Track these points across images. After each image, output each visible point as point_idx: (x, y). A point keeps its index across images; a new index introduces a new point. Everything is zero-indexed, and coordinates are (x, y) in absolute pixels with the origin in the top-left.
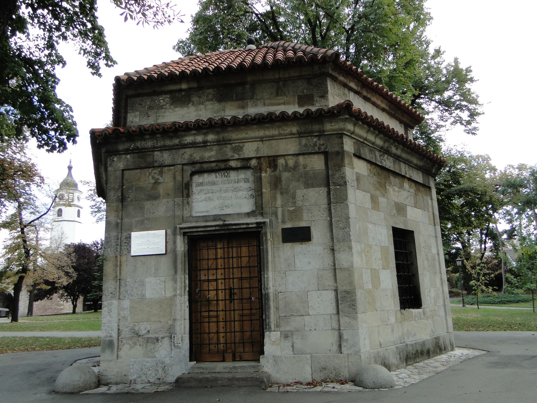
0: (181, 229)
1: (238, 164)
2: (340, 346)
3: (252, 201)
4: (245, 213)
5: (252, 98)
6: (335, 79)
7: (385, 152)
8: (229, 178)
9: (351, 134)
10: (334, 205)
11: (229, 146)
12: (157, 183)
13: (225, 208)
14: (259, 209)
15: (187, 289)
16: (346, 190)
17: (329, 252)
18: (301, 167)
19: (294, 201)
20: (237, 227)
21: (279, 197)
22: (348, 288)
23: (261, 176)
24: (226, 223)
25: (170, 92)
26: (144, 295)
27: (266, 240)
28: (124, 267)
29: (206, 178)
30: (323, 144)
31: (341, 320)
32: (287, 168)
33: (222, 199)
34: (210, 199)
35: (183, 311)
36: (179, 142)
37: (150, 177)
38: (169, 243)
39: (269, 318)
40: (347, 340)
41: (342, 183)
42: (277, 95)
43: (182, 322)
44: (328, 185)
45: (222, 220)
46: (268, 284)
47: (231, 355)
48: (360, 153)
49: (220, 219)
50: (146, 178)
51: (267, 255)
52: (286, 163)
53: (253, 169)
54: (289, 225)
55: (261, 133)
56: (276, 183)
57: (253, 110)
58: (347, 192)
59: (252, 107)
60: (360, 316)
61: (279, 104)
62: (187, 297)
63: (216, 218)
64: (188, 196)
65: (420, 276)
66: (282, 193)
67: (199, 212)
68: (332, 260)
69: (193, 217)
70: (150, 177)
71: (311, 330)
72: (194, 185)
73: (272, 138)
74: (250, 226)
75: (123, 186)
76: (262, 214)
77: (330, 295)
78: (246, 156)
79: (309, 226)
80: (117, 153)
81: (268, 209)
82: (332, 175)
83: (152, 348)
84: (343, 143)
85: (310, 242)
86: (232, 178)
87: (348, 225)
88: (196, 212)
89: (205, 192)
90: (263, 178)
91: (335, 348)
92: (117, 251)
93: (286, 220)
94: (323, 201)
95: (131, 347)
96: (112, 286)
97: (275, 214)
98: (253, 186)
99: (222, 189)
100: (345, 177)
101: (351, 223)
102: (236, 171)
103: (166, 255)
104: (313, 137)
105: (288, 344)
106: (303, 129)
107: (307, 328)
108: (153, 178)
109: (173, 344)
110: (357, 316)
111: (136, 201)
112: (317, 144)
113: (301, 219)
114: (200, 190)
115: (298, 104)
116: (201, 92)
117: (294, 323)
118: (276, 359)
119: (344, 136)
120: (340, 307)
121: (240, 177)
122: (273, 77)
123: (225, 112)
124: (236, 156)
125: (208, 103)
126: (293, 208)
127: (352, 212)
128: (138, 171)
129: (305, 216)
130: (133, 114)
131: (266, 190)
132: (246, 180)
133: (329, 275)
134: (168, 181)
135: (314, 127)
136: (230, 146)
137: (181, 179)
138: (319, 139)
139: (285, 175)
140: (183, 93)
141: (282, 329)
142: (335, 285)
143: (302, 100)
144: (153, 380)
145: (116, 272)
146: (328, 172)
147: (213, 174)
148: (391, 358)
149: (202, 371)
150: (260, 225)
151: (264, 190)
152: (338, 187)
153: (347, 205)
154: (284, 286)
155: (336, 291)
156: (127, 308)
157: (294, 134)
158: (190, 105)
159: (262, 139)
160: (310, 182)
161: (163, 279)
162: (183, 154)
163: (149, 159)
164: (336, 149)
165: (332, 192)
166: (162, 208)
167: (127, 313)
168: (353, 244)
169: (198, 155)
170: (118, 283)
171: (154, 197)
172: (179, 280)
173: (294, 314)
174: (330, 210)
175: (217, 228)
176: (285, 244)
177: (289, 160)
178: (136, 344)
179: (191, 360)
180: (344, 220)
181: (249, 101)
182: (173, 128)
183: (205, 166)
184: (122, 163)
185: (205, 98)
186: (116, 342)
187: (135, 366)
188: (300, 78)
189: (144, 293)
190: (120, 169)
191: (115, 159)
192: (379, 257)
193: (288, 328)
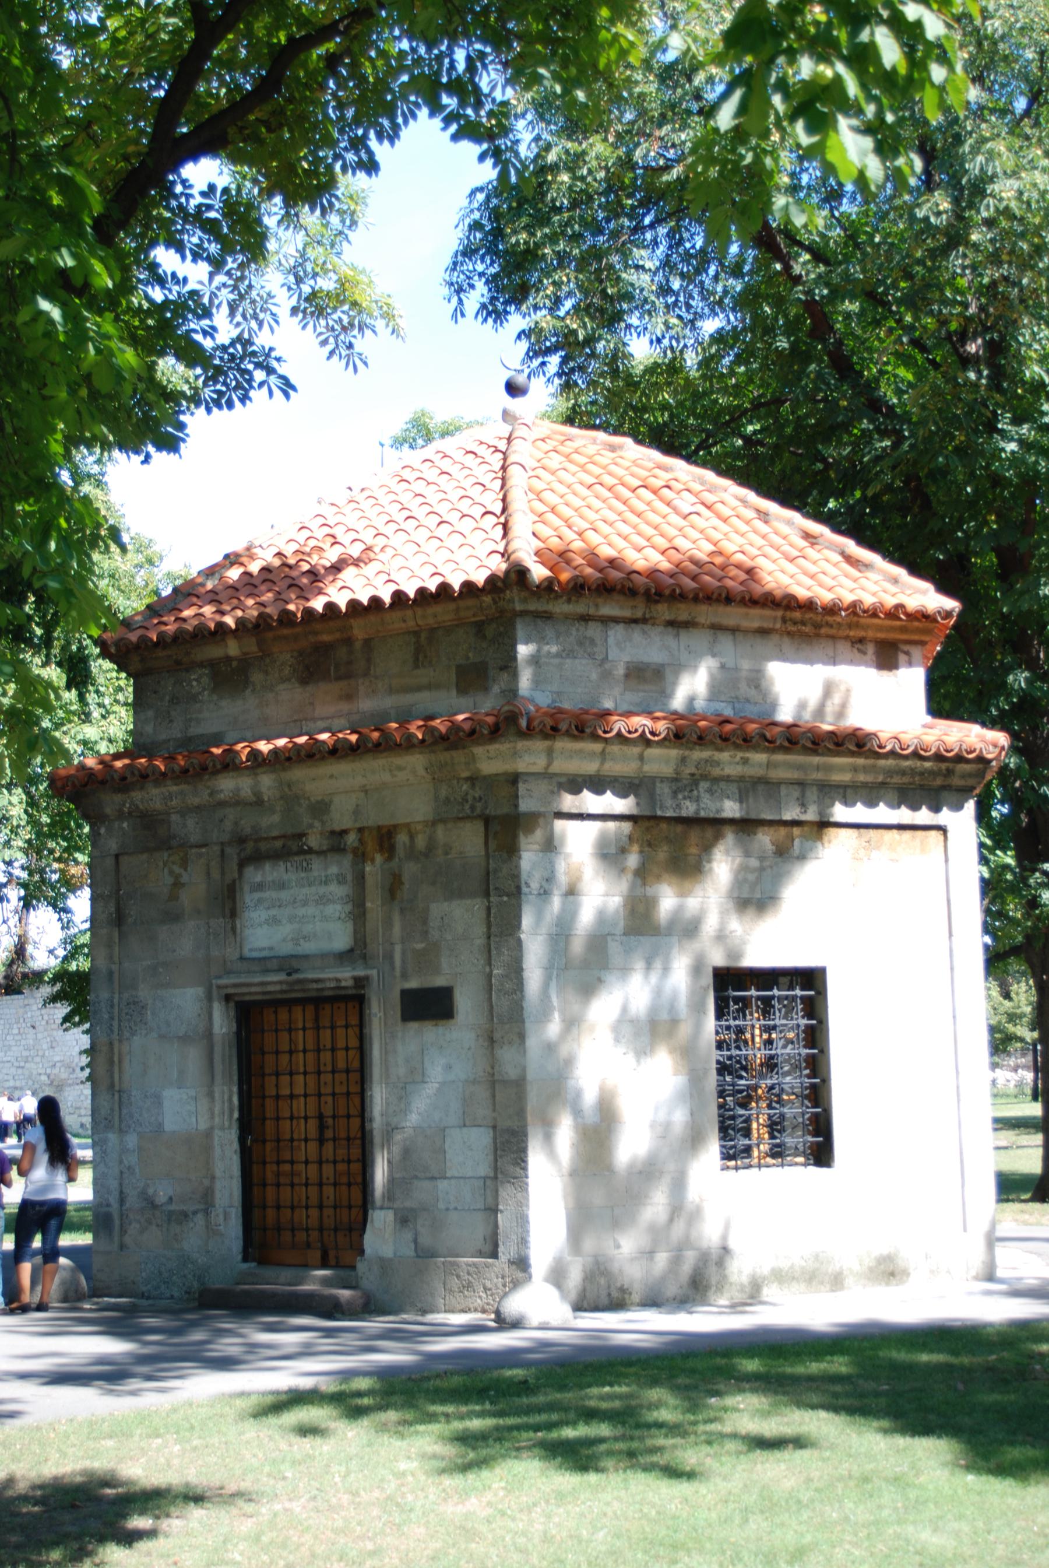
0: (219, 987)
5: (366, 674)
12: (177, 884)
13: (302, 941)
15: (236, 1115)
18: (440, 851)
20: (320, 986)
25: (212, 664)
26: (161, 1125)
30: (480, 798)
34: (275, 921)
36: (211, 795)
42: (416, 666)
44: (487, 894)
47: (318, 1254)
54: (413, 984)
56: (393, 888)
61: (419, 688)
64: (233, 914)
66: (402, 911)
72: (247, 888)
76: (364, 957)
82: (496, 871)
84: (517, 797)
86: (316, 874)
88: (251, 950)
94: (479, 931)
97: (389, 957)
107: (441, 1205)
108: (171, 872)
112: (470, 798)
113: (437, 971)
125: (281, 687)
128: (145, 856)
129: (445, 962)
131: (374, 904)
132: (341, 880)
133: (482, 1093)
139: (410, 869)
145: (112, 1077)
150: (361, 982)
151: (368, 905)
152: (505, 899)
155: (494, 1127)
158: (248, 692)
165: (493, 911)
166: (185, 941)
167: (132, 1159)
171: (173, 917)
172: (217, 1095)
179: (245, 1259)
181: (360, 681)
183: (263, 846)
193: (408, 1204)
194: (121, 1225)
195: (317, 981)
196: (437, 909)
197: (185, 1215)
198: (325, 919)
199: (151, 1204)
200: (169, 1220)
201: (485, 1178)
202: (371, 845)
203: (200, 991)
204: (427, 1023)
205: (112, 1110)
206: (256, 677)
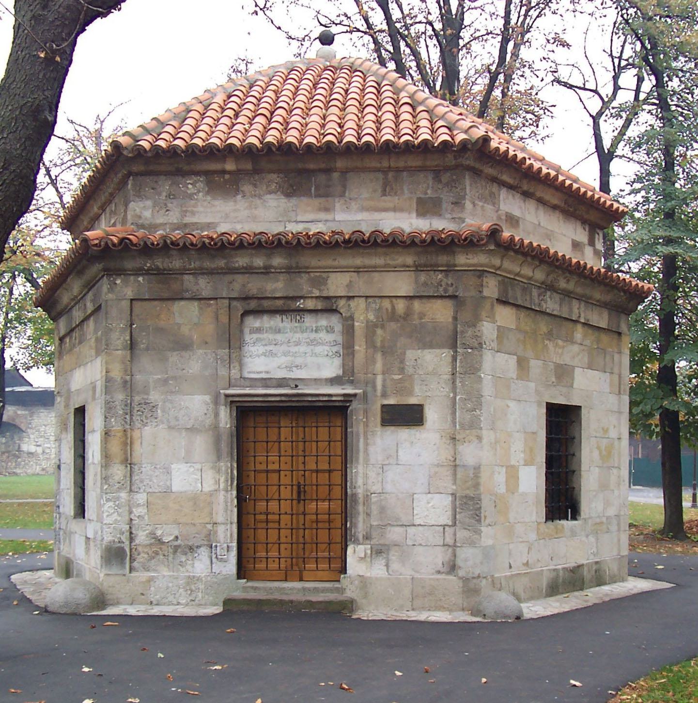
0: (227, 396)
1: (320, 305)
3: (338, 362)
4: (326, 380)
5: (342, 195)
8: (303, 325)
9: (496, 270)
10: (462, 376)
11: (305, 277)
13: (294, 369)
16: (481, 356)
17: (448, 442)
18: (416, 316)
19: (402, 366)
23: (353, 326)
25: (207, 173)
30: (452, 284)
33: (292, 356)
34: (271, 354)
35: (229, 512)
39: (356, 527)
41: (476, 345)
42: (384, 194)
43: (229, 526)
46: (356, 483)
51: (358, 441)
54: (391, 401)
55: (358, 261)
62: (235, 493)
63: (282, 382)
67: (254, 372)
68: (452, 453)
69: (244, 378)
71: (414, 545)
72: (246, 330)
73: (374, 269)
74: (334, 399)
75: (131, 325)
76: (352, 382)
81: (360, 376)
82: (462, 332)
85: (421, 427)
86: (307, 324)
88: (249, 372)
90: (356, 328)
92: (126, 422)
93: (389, 393)
96: (119, 472)
98: (340, 339)
99: (291, 341)
104: (437, 273)
106: (423, 260)
109: (214, 556)
112: (443, 284)
113: (411, 393)
114: (257, 339)
116: (257, 177)
120: (457, 517)
122: (378, 165)
123: (297, 215)
124: (317, 293)
125: (268, 196)
126: (400, 376)
127: (487, 388)
129: (417, 389)
130: (141, 204)
131: (360, 347)
132: (330, 330)
133: (446, 473)
135: (440, 258)
136: (307, 276)
138: (447, 276)
140: (227, 176)
147: (278, 316)
150: (349, 398)
151: (357, 348)
152: (470, 351)
154: (380, 484)
157: (408, 267)
158: (239, 197)
159: (358, 270)
161: (198, 466)
162: (231, 283)
163: (175, 286)
165: (459, 358)
166: (195, 364)
168: (485, 433)
169: (254, 285)
170: (129, 468)
174: (454, 382)
175: (283, 399)
181: (337, 200)
183: (266, 304)
188: (423, 169)
194: (131, 555)
196: (411, 355)
200: (175, 552)
201: (444, 526)
203: (207, 398)
204: (400, 427)
205: (125, 477)
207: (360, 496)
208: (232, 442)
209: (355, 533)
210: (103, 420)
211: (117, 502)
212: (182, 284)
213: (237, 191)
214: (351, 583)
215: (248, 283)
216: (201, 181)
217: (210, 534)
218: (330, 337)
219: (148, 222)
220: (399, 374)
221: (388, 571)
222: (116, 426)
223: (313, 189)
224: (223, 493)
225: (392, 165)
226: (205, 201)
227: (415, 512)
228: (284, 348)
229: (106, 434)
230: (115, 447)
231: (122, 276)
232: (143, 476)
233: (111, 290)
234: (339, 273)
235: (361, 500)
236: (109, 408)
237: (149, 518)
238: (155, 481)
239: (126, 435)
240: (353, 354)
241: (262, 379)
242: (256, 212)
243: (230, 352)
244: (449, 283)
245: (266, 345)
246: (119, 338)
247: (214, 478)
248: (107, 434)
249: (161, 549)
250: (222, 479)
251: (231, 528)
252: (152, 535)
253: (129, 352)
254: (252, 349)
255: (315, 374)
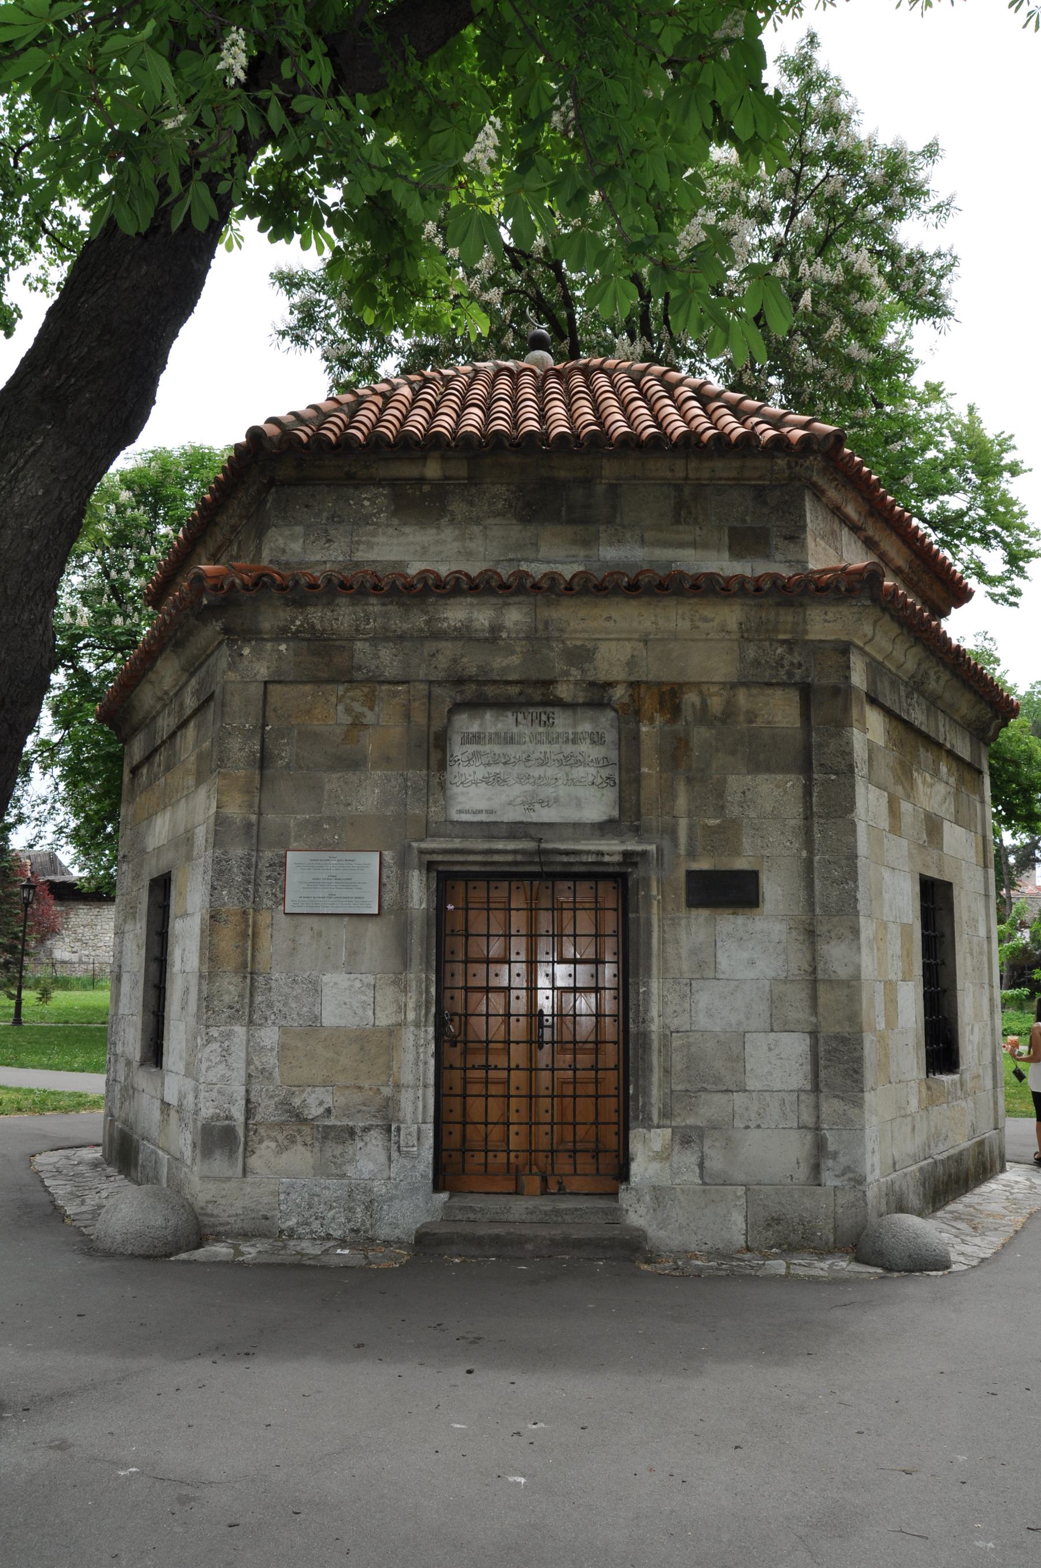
0: (422, 852)
2: (816, 1169)
3: (610, 795)
4: (593, 825)
5: (610, 521)
6: (818, 494)
7: (917, 686)
13: (537, 806)
14: (629, 817)
15: (433, 1010)
16: (853, 787)
17: (801, 938)
18: (741, 718)
20: (572, 859)
21: (682, 789)
22: (846, 1030)
23: (638, 731)
24: (543, 845)
25: (393, 483)
26: (317, 1018)
27: (648, 897)
28: (264, 941)
29: (490, 722)
30: (800, 665)
31: (825, 1107)
32: (704, 716)
34: (497, 780)
36: (428, 622)
37: (340, 707)
38: (389, 887)
39: (647, 1093)
40: (835, 1155)
42: (677, 520)
43: (420, 1093)
45: (533, 839)
46: (646, 1011)
47: (537, 1181)
48: (875, 692)
49: (527, 836)
50: (332, 712)
52: (704, 703)
53: (615, 710)
54: (704, 865)
56: (676, 753)
57: (616, 553)
58: (854, 791)
59: (611, 544)
60: (868, 1096)
61: (681, 545)
62: (431, 1030)
63: (516, 830)
64: (443, 766)
65: (959, 994)
66: (689, 781)
67: (467, 812)
68: (809, 957)
69: (452, 822)
70: (340, 707)
71: (747, 1127)
72: (456, 739)
74: (607, 859)
75: (264, 725)
76: (637, 831)
77: (795, 1046)
78: (602, 677)
79: (755, 868)
80: (252, 635)
81: (652, 819)
83: (337, 1153)
84: (848, 667)
85: (756, 911)
86: (560, 730)
87: (852, 874)
88: (460, 812)
89: (485, 760)
90: (643, 737)
91: (803, 1173)
92: (247, 897)
94: (793, 811)
95: (281, 1149)
96: (231, 988)
98: (614, 755)
99: (533, 757)
100: (850, 753)
101: (860, 871)
102: (569, 712)
103: (378, 919)
105: (689, 1158)
107: (739, 1123)
108: (348, 710)
109: (394, 1147)
110: (862, 1098)
111: (301, 768)
112: (785, 662)
114: (473, 754)
115: (730, 548)
116: (474, 491)
117: (711, 1107)
118: (659, 1194)
119: (853, 650)
121: (580, 729)
123: (538, 551)
125: (491, 521)
126: (718, 821)
128: (308, 688)
129: (746, 842)
132: (597, 739)
133: (798, 995)
134: (386, 725)
137: (424, 721)
139: (700, 735)
141: (677, 1122)
142: (813, 1019)
143: (746, 541)
144: (340, 1232)
145: (244, 954)
146: (808, 736)
147: (510, 714)
148: (911, 1195)
149: (472, 1216)
151: (645, 770)
152: (833, 777)
153: (853, 824)
154: (687, 1015)
155: (814, 1034)
156: (272, 1049)
158: (444, 521)
160: (762, 757)
161: (370, 979)
162: (433, 655)
164: (833, 680)
165: (816, 790)
166: (369, 794)
167: (271, 1060)
168: (862, 919)
170: (248, 981)
173: (709, 1087)
174: (808, 832)
175: (519, 858)
176: (694, 912)
177: (711, 695)
178: (294, 1142)
180: (844, 862)
181: (602, 528)
182: (420, 586)
183: (490, 691)
184: (265, 664)
185: (485, 508)
186: (241, 1131)
187: (293, 1196)
189: (317, 1012)
190: (259, 677)
191: (246, 651)
192: (899, 953)
193: (691, 1121)
194: (246, 1143)
195: (567, 853)
197: (351, 1132)
198: (573, 782)
199: (298, 1117)
200: (325, 1138)
202: (649, 704)
204: (721, 910)
205: (241, 996)
206: (457, 507)
207: (654, 1037)
208: (428, 937)
209: (644, 1105)
210: (208, 893)
211: (227, 1043)
212: (352, 657)
213: (443, 511)
214: (639, 1200)
215: (462, 656)
216: (385, 496)
217: (386, 1107)
218: (594, 752)
219: (296, 559)
220: (716, 818)
221: (702, 1178)
222: (231, 902)
223: (564, 509)
224: (412, 1028)
225: (691, 475)
226: (388, 526)
227: (748, 1067)
228: (519, 769)
229: (212, 917)
230: (227, 940)
231: (253, 643)
232: (274, 996)
233: (232, 666)
234: (614, 643)
235: (655, 1045)
236: (220, 872)
237: (282, 1075)
238: (294, 1005)
239: (247, 921)
240: (638, 780)
241: (481, 823)
242: (471, 545)
243: (428, 775)
244: (795, 661)
245: (489, 764)
246: (240, 749)
247: (397, 1001)
248: (214, 917)
249: (299, 1131)
250: (411, 1004)
251: (424, 1095)
252: (285, 1105)
253: (257, 772)
254: (464, 770)
255: (571, 815)
